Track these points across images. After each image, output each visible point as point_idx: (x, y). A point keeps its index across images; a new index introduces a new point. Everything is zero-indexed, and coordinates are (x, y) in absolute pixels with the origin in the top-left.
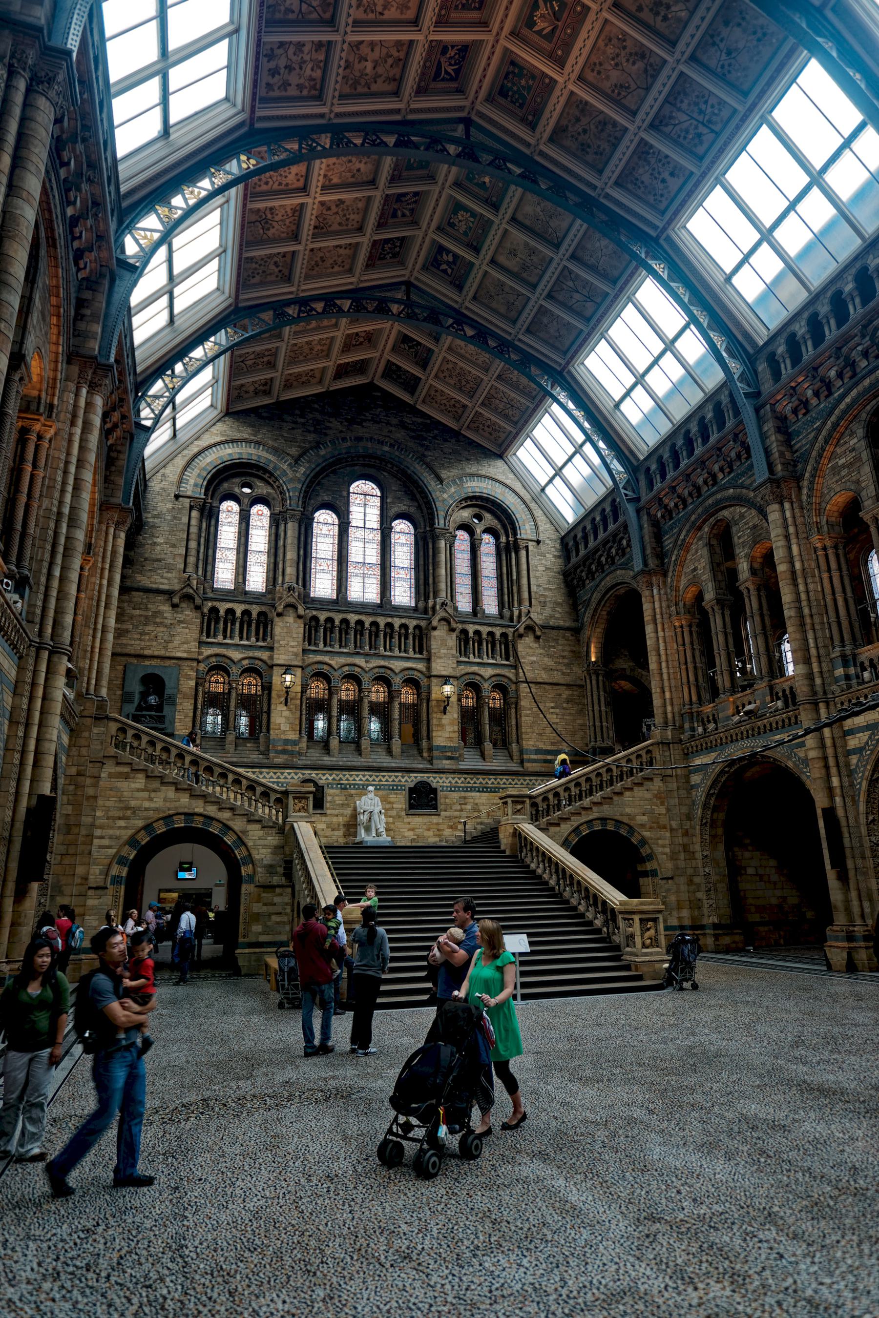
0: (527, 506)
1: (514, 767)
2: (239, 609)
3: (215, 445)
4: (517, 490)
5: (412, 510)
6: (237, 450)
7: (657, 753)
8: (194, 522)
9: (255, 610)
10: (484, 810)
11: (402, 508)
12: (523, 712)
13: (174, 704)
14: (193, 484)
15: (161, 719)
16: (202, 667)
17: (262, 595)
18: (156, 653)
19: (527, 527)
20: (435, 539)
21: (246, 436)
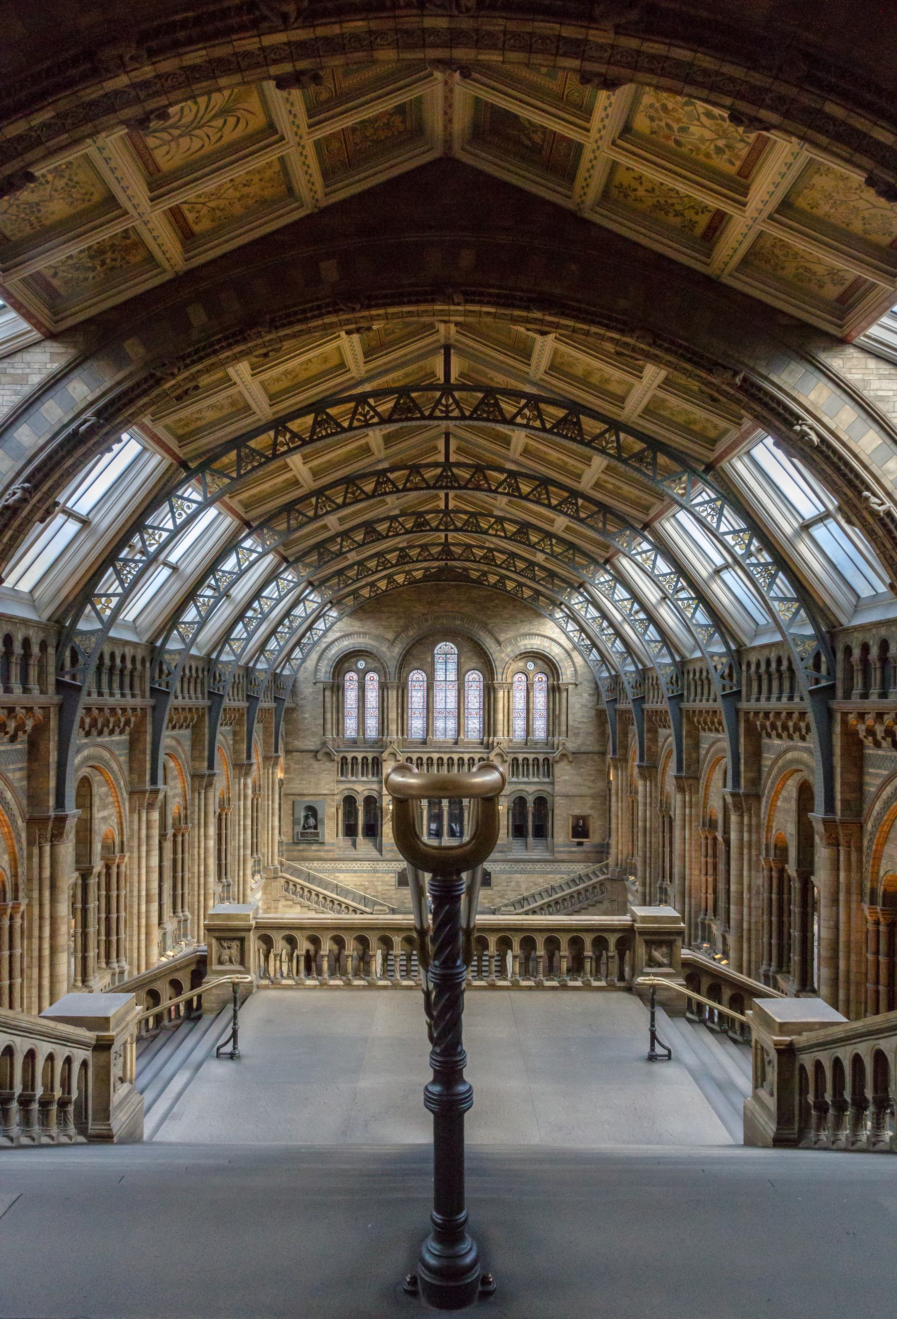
0: (569, 655)
1: (547, 856)
2: (360, 756)
3: (336, 640)
4: (561, 642)
5: (480, 665)
6: (352, 641)
7: (608, 885)
8: (328, 699)
9: (370, 756)
10: (524, 886)
11: (473, 665)
12: (556, 818)
13: (323, 824)
14: (324, 672)
15: (317, 834)
16: (339, 798)
17: (376, 742)
18: (312, 792)
19: (568, 672)
20: (495, 690)
21: (357, 629)
